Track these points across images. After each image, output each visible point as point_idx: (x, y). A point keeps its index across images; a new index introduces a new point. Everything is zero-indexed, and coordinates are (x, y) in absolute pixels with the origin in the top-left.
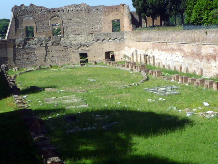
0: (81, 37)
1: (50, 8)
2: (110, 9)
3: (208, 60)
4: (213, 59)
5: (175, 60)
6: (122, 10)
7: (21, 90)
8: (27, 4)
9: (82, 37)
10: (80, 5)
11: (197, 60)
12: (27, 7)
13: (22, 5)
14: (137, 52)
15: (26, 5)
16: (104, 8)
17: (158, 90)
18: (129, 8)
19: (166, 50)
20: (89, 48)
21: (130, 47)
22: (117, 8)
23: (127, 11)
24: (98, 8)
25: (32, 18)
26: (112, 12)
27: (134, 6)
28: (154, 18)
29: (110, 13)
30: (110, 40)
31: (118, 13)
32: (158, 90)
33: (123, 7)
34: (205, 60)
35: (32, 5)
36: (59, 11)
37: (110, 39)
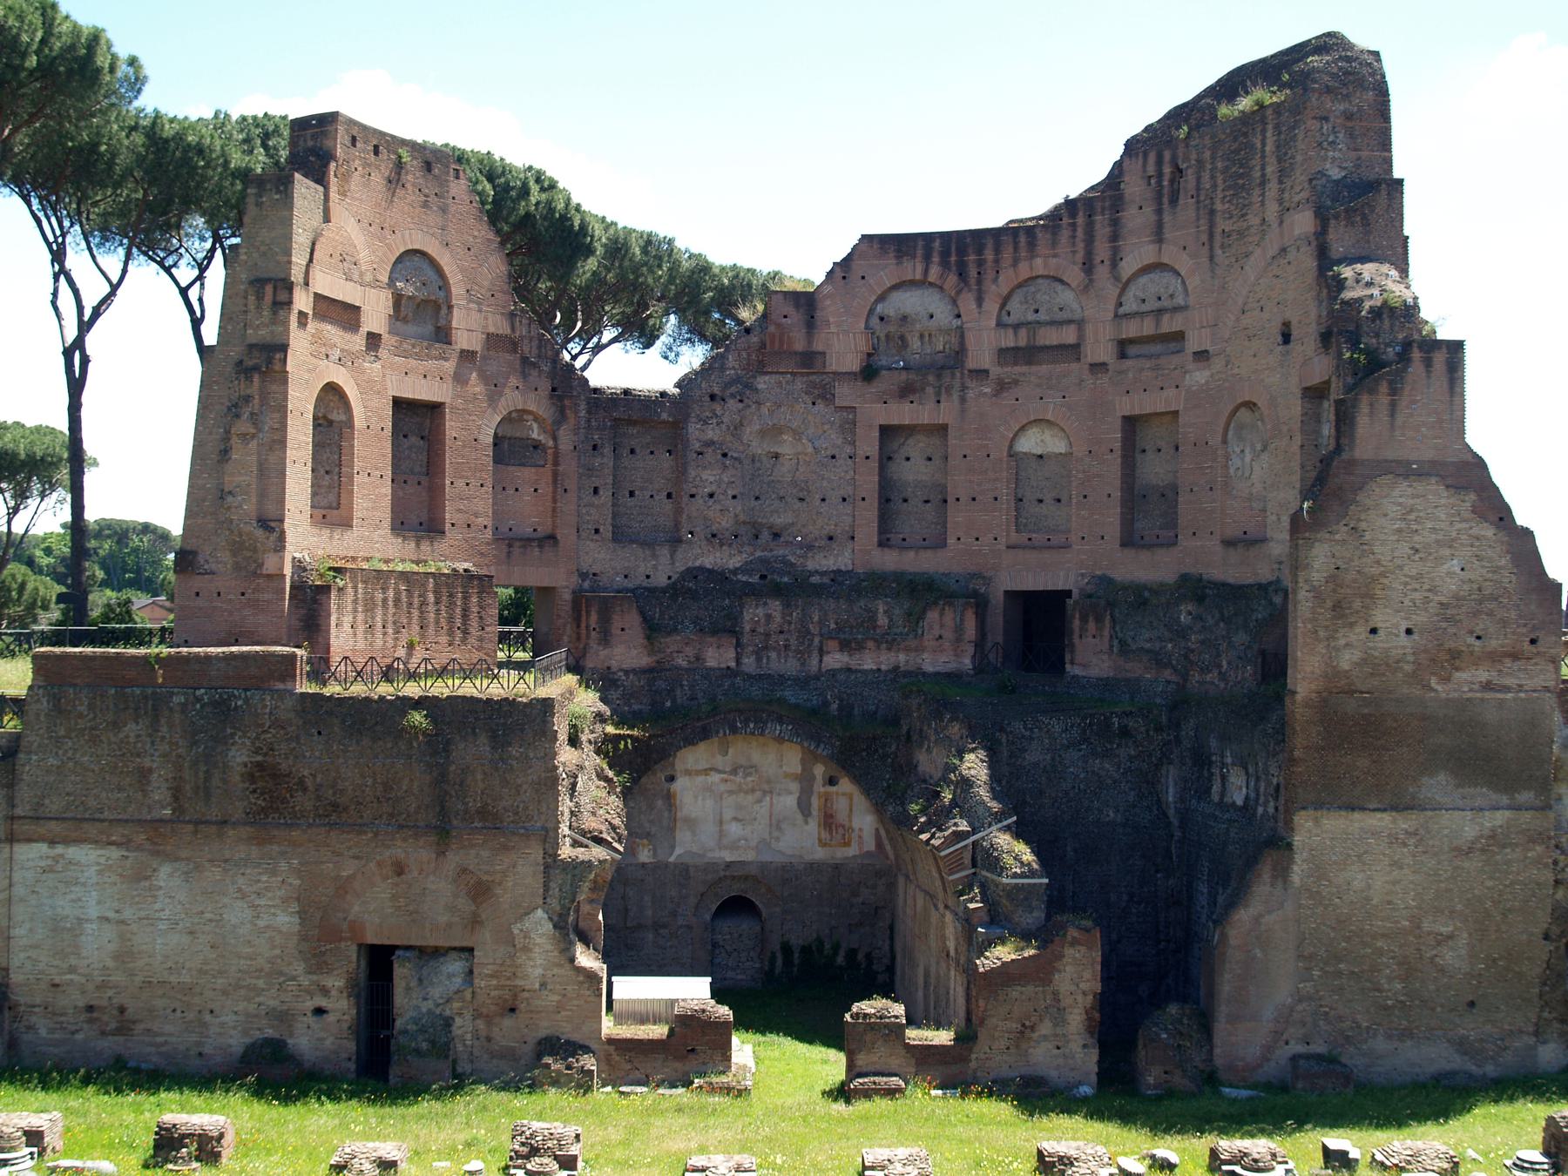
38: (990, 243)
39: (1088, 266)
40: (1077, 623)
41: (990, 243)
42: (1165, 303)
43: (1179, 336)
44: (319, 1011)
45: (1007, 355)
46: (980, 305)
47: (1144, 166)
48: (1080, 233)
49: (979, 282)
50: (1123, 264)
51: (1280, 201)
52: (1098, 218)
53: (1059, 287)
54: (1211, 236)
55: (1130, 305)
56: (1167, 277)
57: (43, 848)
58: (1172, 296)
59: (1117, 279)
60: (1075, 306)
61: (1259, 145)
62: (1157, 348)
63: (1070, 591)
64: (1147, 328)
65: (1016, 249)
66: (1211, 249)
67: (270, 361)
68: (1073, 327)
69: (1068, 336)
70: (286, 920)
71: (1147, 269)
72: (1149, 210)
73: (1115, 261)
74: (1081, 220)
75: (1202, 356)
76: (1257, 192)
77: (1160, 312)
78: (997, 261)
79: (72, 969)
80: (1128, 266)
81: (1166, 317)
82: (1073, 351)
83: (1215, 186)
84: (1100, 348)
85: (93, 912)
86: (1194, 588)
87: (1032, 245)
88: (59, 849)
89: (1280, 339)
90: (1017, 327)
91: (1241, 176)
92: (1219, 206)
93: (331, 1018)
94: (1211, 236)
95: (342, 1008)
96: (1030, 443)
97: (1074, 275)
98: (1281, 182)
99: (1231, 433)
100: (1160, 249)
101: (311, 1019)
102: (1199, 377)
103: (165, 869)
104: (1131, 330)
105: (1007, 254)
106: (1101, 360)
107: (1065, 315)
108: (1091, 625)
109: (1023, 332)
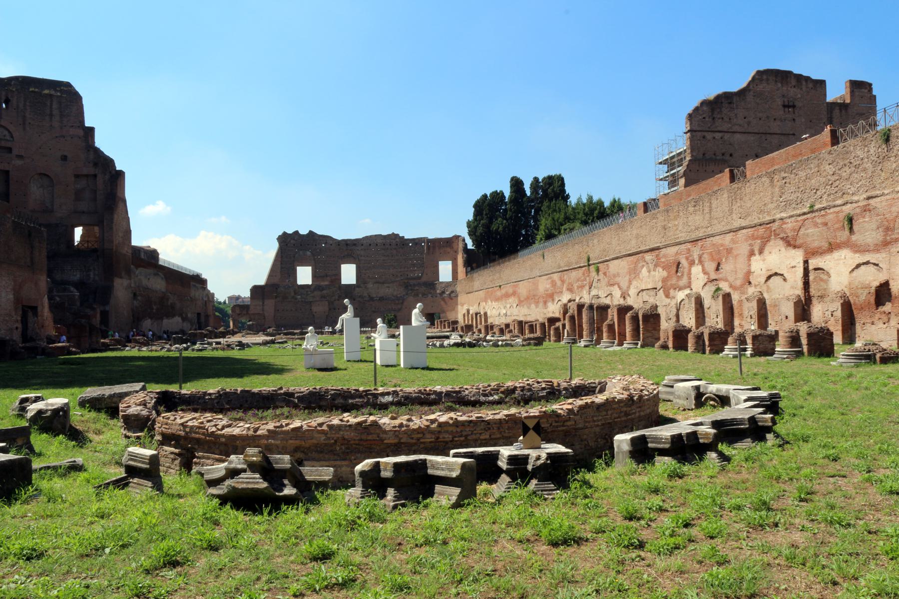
1: (340, 239)
3: (545, 303)
4: (551, 300)
5: (508, 314)
6: (455, 245)
7: (165, 317)
8: (304, 231)
9: (389, 287)
11: (533, 306)
12: (304, 235)
13: (296, 233)
14: (468, 311)
18: (464, 240)
19: (497, 299)
20: (399, 306)
21: (462, 305)
23: (461, 245)
24: (417, 241)
25: (309, 253)
27: (471, 234)
31: (448, 249)
34: (541, 305)
35: (311, 233)
36: (355, 245)
44: (17, 328)
61: (49, 104)
70: (11, 296)
93: (19, 330)
95: (19, 325)
99: (32, 181)
101: (15, 331)
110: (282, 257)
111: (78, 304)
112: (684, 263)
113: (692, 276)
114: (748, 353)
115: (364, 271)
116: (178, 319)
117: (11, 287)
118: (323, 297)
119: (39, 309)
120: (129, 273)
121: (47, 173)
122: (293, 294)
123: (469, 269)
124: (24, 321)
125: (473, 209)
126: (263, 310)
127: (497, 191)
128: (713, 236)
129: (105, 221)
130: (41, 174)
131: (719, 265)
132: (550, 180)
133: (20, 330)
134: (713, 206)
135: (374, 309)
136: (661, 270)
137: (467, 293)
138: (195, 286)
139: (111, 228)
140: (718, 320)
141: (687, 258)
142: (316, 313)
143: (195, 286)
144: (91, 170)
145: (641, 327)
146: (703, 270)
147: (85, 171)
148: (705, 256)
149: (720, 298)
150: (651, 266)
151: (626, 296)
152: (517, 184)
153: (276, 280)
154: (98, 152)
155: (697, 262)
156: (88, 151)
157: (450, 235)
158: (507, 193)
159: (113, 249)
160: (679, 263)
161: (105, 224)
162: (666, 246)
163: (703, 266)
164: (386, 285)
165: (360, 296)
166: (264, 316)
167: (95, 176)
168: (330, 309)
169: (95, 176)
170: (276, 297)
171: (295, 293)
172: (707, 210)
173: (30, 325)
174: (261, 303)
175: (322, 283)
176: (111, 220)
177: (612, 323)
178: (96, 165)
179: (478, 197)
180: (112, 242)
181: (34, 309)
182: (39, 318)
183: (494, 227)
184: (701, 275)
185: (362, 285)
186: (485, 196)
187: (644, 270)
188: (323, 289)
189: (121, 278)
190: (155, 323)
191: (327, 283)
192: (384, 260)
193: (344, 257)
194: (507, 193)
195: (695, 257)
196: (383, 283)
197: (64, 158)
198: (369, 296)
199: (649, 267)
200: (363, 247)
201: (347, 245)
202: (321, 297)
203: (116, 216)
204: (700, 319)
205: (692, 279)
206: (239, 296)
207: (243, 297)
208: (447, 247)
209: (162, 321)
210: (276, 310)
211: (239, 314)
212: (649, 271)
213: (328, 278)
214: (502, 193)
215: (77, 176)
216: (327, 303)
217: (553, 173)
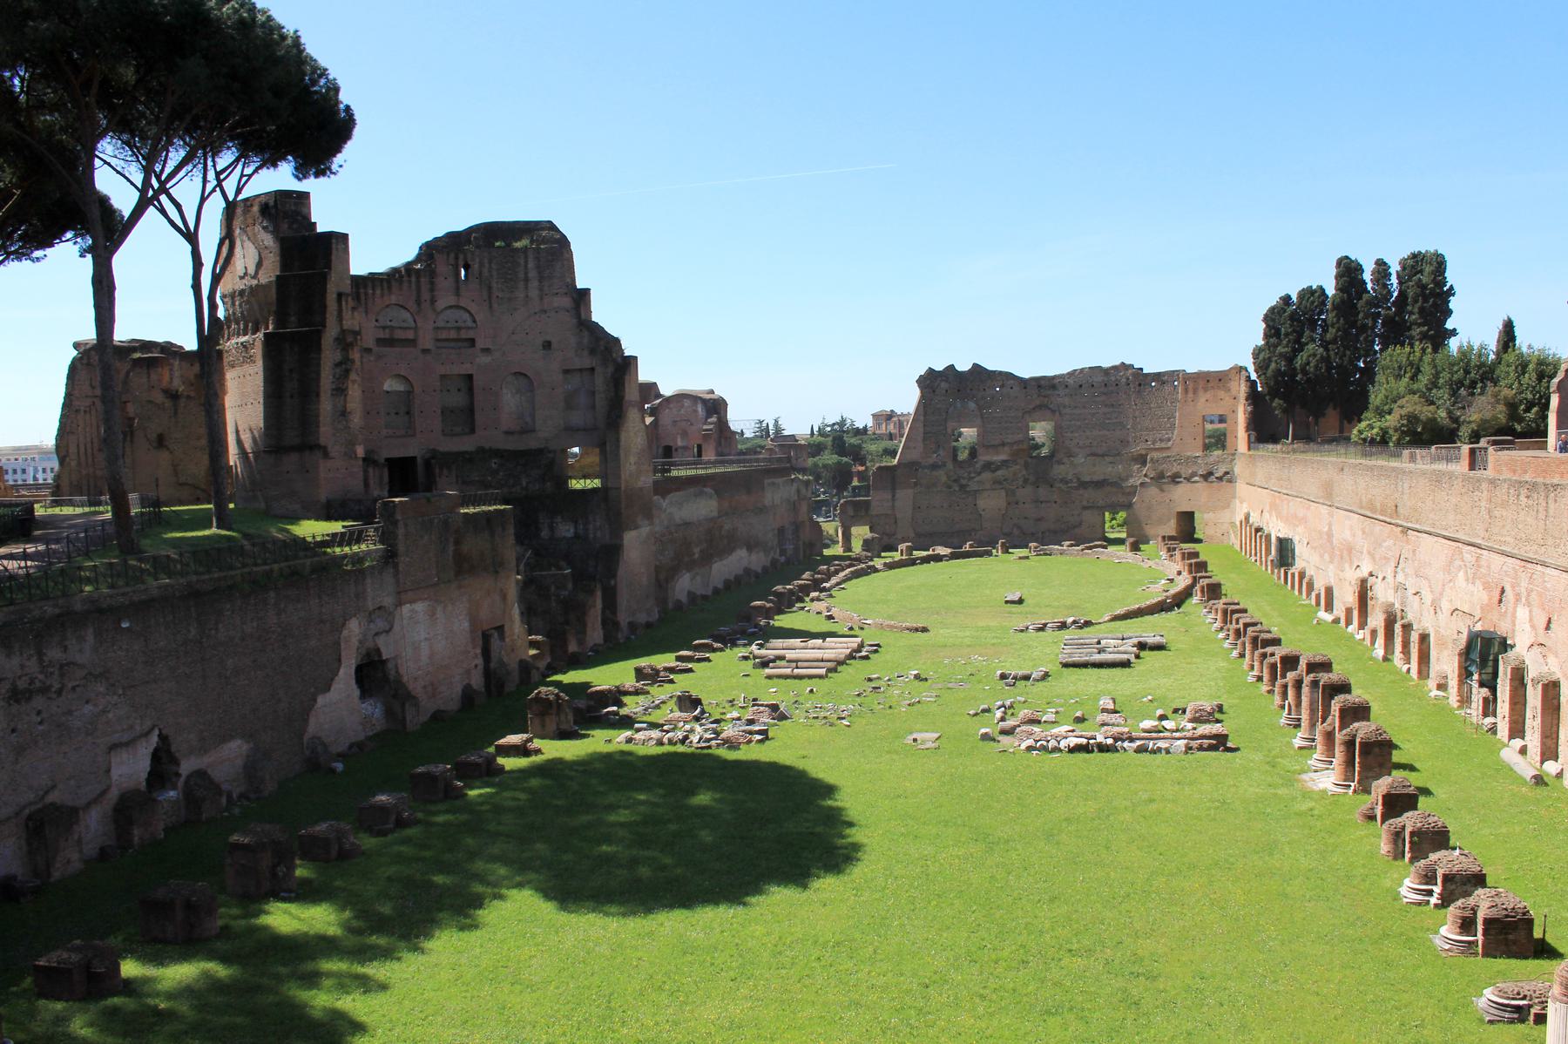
0: (1111, 465)
1: (1026, 375)
2: (1201, 383)
6: (1233, 385)
8: (963, 366)
10: (1114, 368)
13: (951, 367)
15: (960, 368)
16: (1184, 378)
17: (1099, 643)
22: (1220, 380)
23: (1243, 389)
25: (972, 405)
26: (1205, 390)
27: (1256, 371)
28: (1319, 414)
29: (1201, 393)
30: (1196, 478)
31: (1221, 394)
32: (1099, 643)
33: (1237, 378)
35: (976, 366)
37: (1194, 474)
38: (370, 284)
39: (418, 302)
40: (437, 471)
41: (370, 284)
42: (463, 325)
43: (472, 342)
45: (381, 342)
46: (366, 315)
47: (448, 259)
48: (413, 286)
49: (366, 304)
50: (436, 303)
51: (541, 290)
52: (422, 280)
53: (403, 311)
54: (490, 297)
55: (441, 324)
56: (462, 312)
57: (408, 605)
58: (465, 322)
59: (434, 310)
60: (411, 320)
62: (452, 344)
63: (415, 457)
64: (453, 334)
65: (382, 289)
66: (490, 303)
67: (356, 339)
68: (412, 332)
69: (410, 335)
70: (466, 624)
71: (451, 307)
72: (451, 279)
73: (433, 301)
74: (413, 279)
75: (486, 351)
76: (521, 285)
77: (459, 329)
78: (373, 294)
79: (419, 669)
80: (441, 304)
81: (463, 331)
82: (412, 343)
83: (491, 276)
84: (427, 341)
85: (422, 637)
86: (484, 454)
87: (390, 288)
88: (413, 605)
89: (541, 348)
90: (384, 328)
91: (510, 274)
92: (494, 285)
94: (490, 297)
95: (480, 661)
96: (386, 387)
97: (411, 305)
98: (540, 281)
99: (504, 386)
100: (458, 299)
102: (485, 359)
103: (439, 609)
104: (444, 335)
105: (378, 292)
106: (429, 348)
107: (405, 325)
108: (445, 472)
109: (387, 331)
110: (925, 414)
111: (570, 586)
112: (1509, 593)
113: (1517, 623)
114: (1434, 900)
115: (1069, 434)
116: (742, 553)
117: (464, 613)
118: (997, 482)
119: (506, 628)
120: (649, 516)
121: (522, 371)
122: (944, 479)
123: (1253, 439)
124: (486, 653)
125: (1264, 326)
126: (893, 506)
127: (1311, 287)
128: (1544, 564)
129: (608, 444)
130: (515, 373)
131: (1549, 621)
132: (1415, 263)
133: (481, 667)
134: (1551, 512)
135: (1085, 503)
136: (1481, 588)
137: (1247, 484)
138: (774, 484)
139: (617, 456)
140: (1535, 724)
141: (1513, 587)
142: (984, 510)
143: (774, 484)
144: (586, 361)
145: (1357, 760)
146: (1531, 620)
147: (578, 363)
148: (1534, 595)
149: (1540, 686)
150: (1471, 576)
151: (1438, 610)
152: (1348, 271)
153: (915, 455)
154: (597, 332)
155: (1523, 599)
156: (581, 330)
157: (1226, 367)
158: (1331, 291)
159: (620, 488)
160: (1503, 591)
161: (608, 448)
162: (1490, 549)
163: (1530, 611)
164: (1111, 459)
165: (1062, 480)
166: (896, 518)
167: (593, 369)
168: (1009, 504)
169: (593, 369)
170: (916, 484)
171: (948, 477)
172: (1542, 515)
173: (494, 655)
174: (890, 497)
175: (995, 458)
176: (618, 440)
177: (1330, 729)
178: (592, 352)
179: (1273, 300)
180: (620, 477)
181: (500, 629)
182: (507, 640)
183: (1299, 362)
184: (1527, 627)
185: (1065, 460)
186: (1286, 299)
187: (1461, 574)
188: (998, 468)
189: (636, 528)
190: (698, 578)
191: (1003, 457)
192: (1105, 414)
193: (1034, 409)
194: (1331, 291)
195: (1523, 590)
196: (1103, 456)
197: (547, 345)
198: (1078, 479)
199: (1467, 572)
200: (1067, 390)
201: (1039, 386)
202: (994, 483)
203: (623, 436)
204: (1518, 707)
205: (1517, 628)
206: (892, 411)
207: (899, 413)
208: (1219, 388)
209: (711, 568)
210: (917, 508)
211: (853, 517)
212: (1467, 580)
213: (1006, 448)
214: (1322, 289)
215: (566, 372)
216: (1003, 493)
217: (1422, 247)
